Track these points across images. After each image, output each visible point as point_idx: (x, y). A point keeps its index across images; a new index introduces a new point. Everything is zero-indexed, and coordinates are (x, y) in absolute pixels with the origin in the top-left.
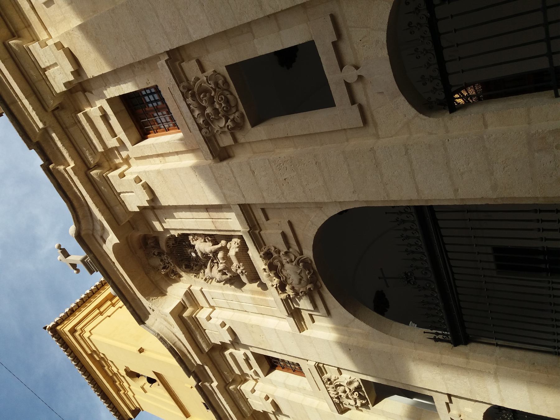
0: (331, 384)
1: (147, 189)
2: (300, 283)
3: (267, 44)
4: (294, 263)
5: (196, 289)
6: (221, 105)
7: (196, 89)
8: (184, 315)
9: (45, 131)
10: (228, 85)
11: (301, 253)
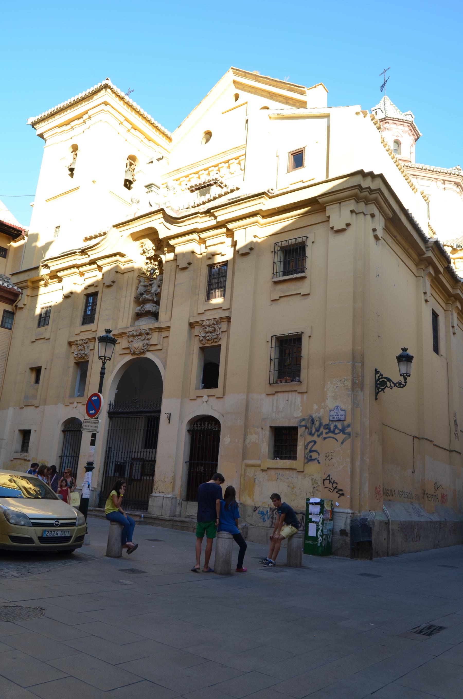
6: (208, 336)
11: (148, 351)
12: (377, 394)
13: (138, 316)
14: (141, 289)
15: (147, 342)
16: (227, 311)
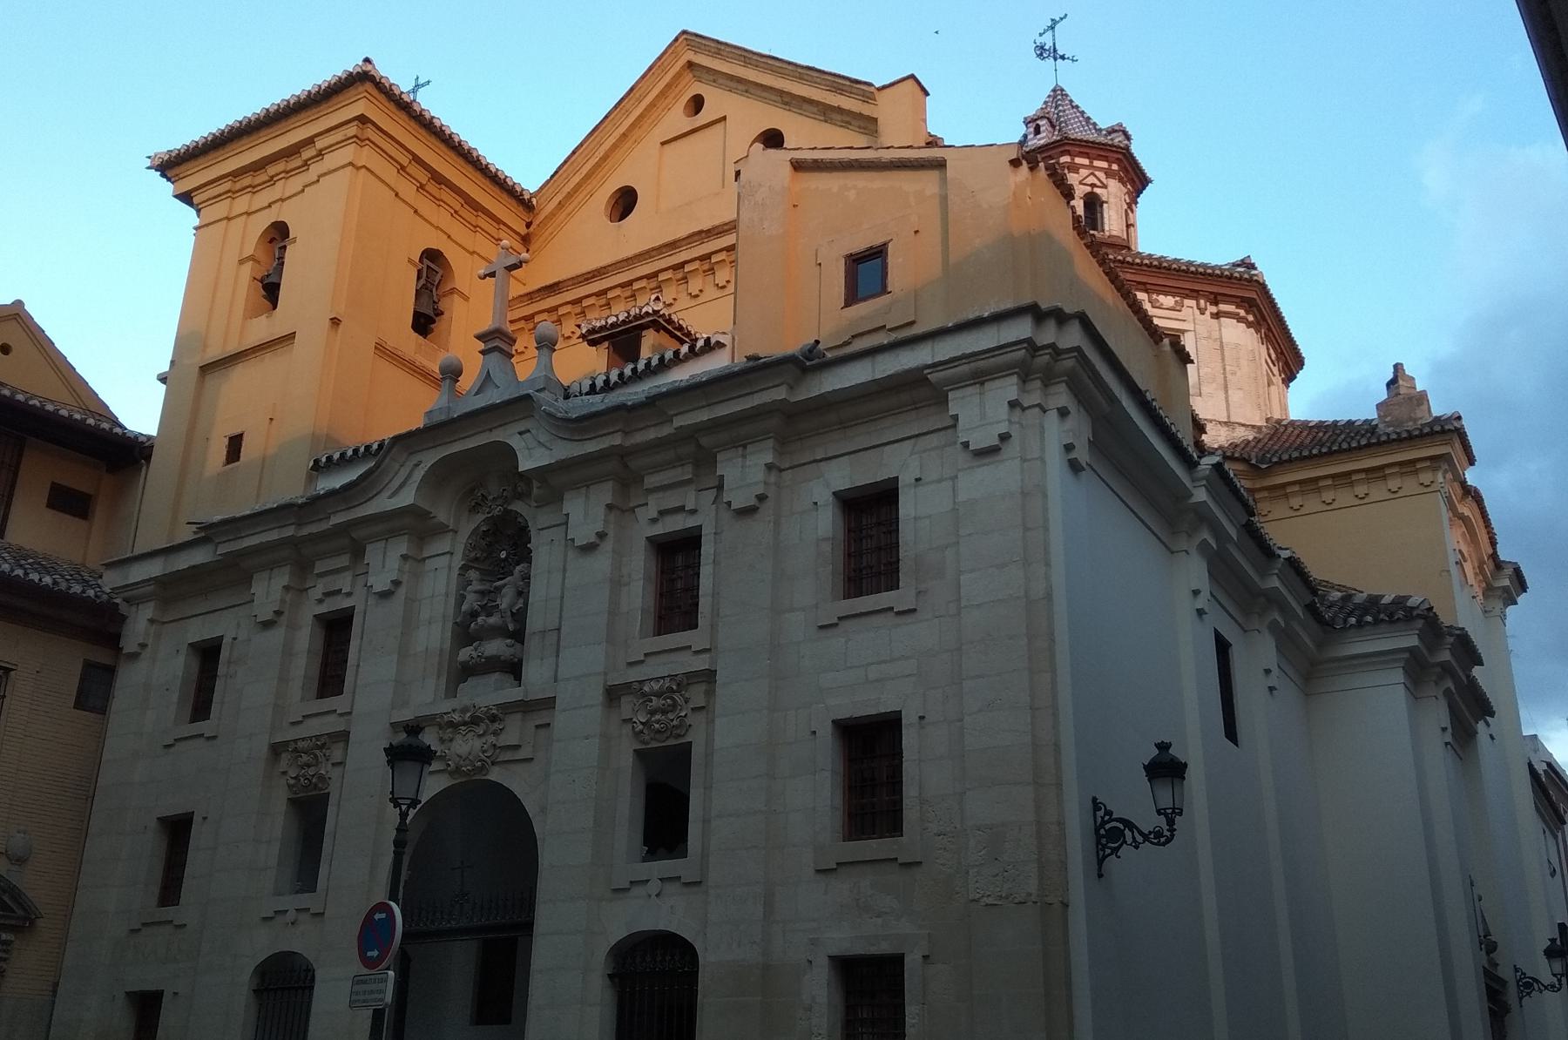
6: (658, 722)
12: (1101, 862)
13: (467, 671)
14: (471, 601)
15: (492, 739)
16: (706, 656)
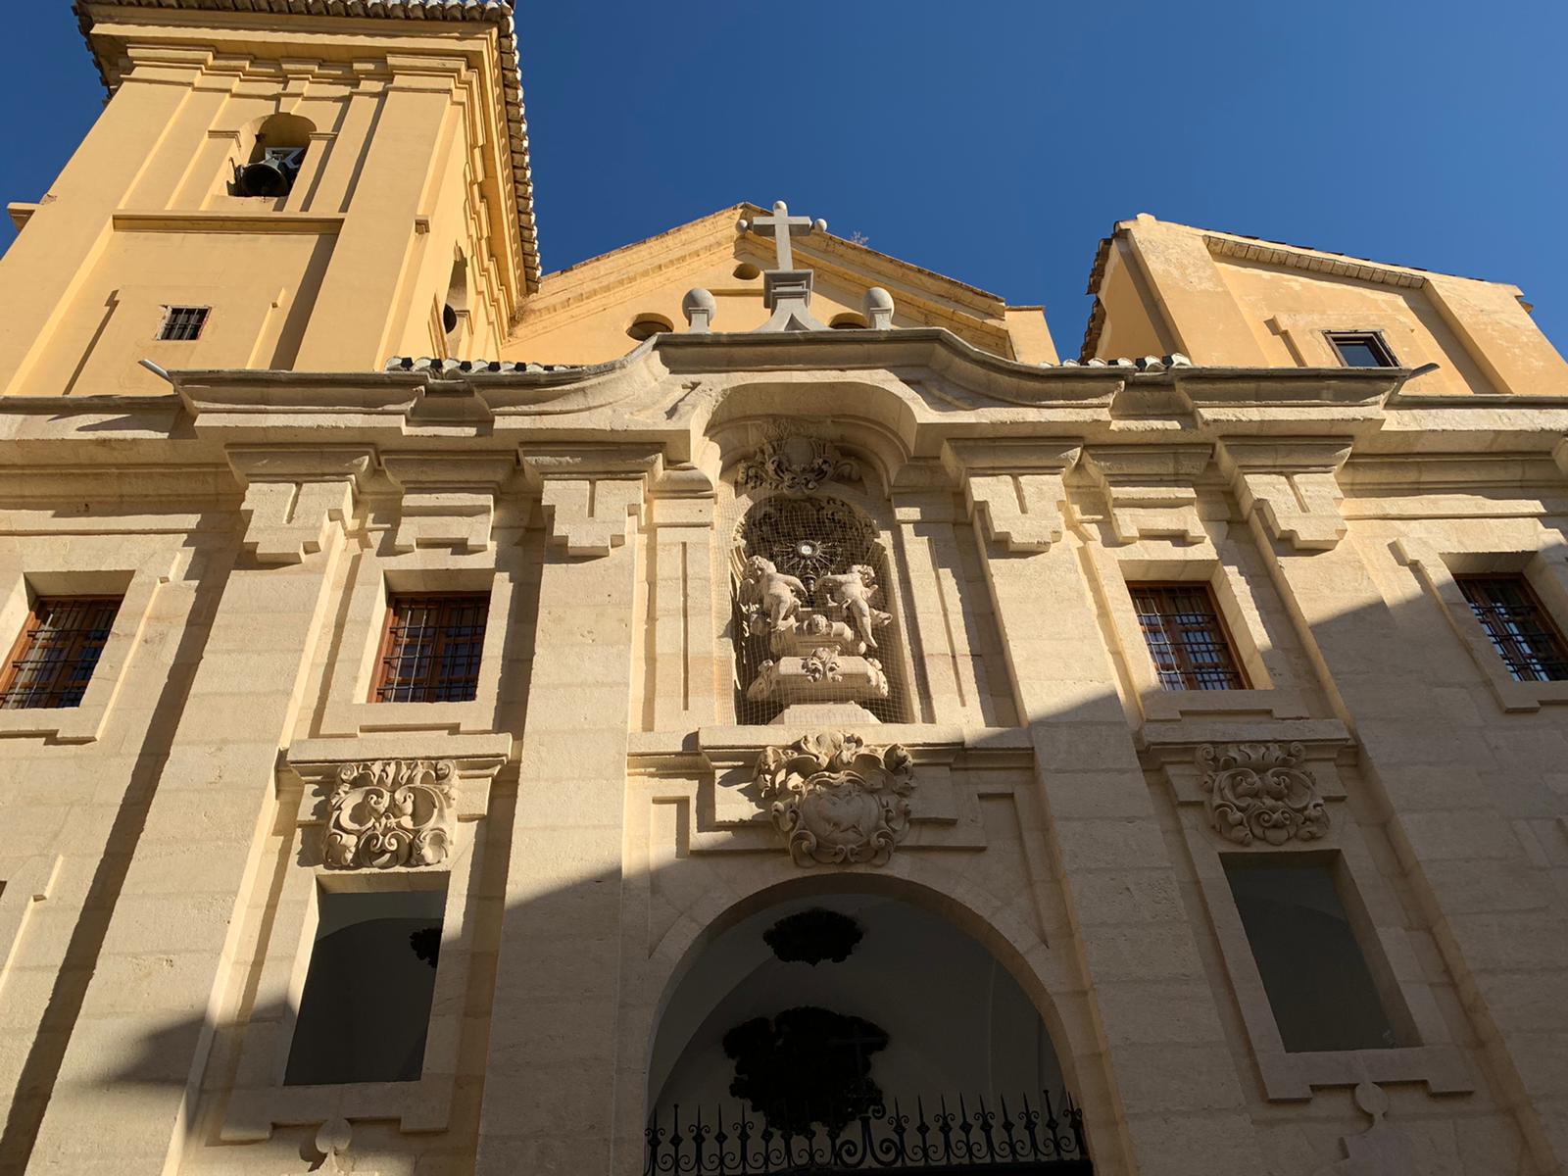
0: (426, 777)
1: (1035, 549)
2: (828, 821)
3: (1396, 949)
4: (883, 823)
5: (713, 512)
7: (1295, 772)
8: (661, 454)
9: (1188, 416)
10: (1305, 840)
11: (899, 849)
15: (892, 801)
